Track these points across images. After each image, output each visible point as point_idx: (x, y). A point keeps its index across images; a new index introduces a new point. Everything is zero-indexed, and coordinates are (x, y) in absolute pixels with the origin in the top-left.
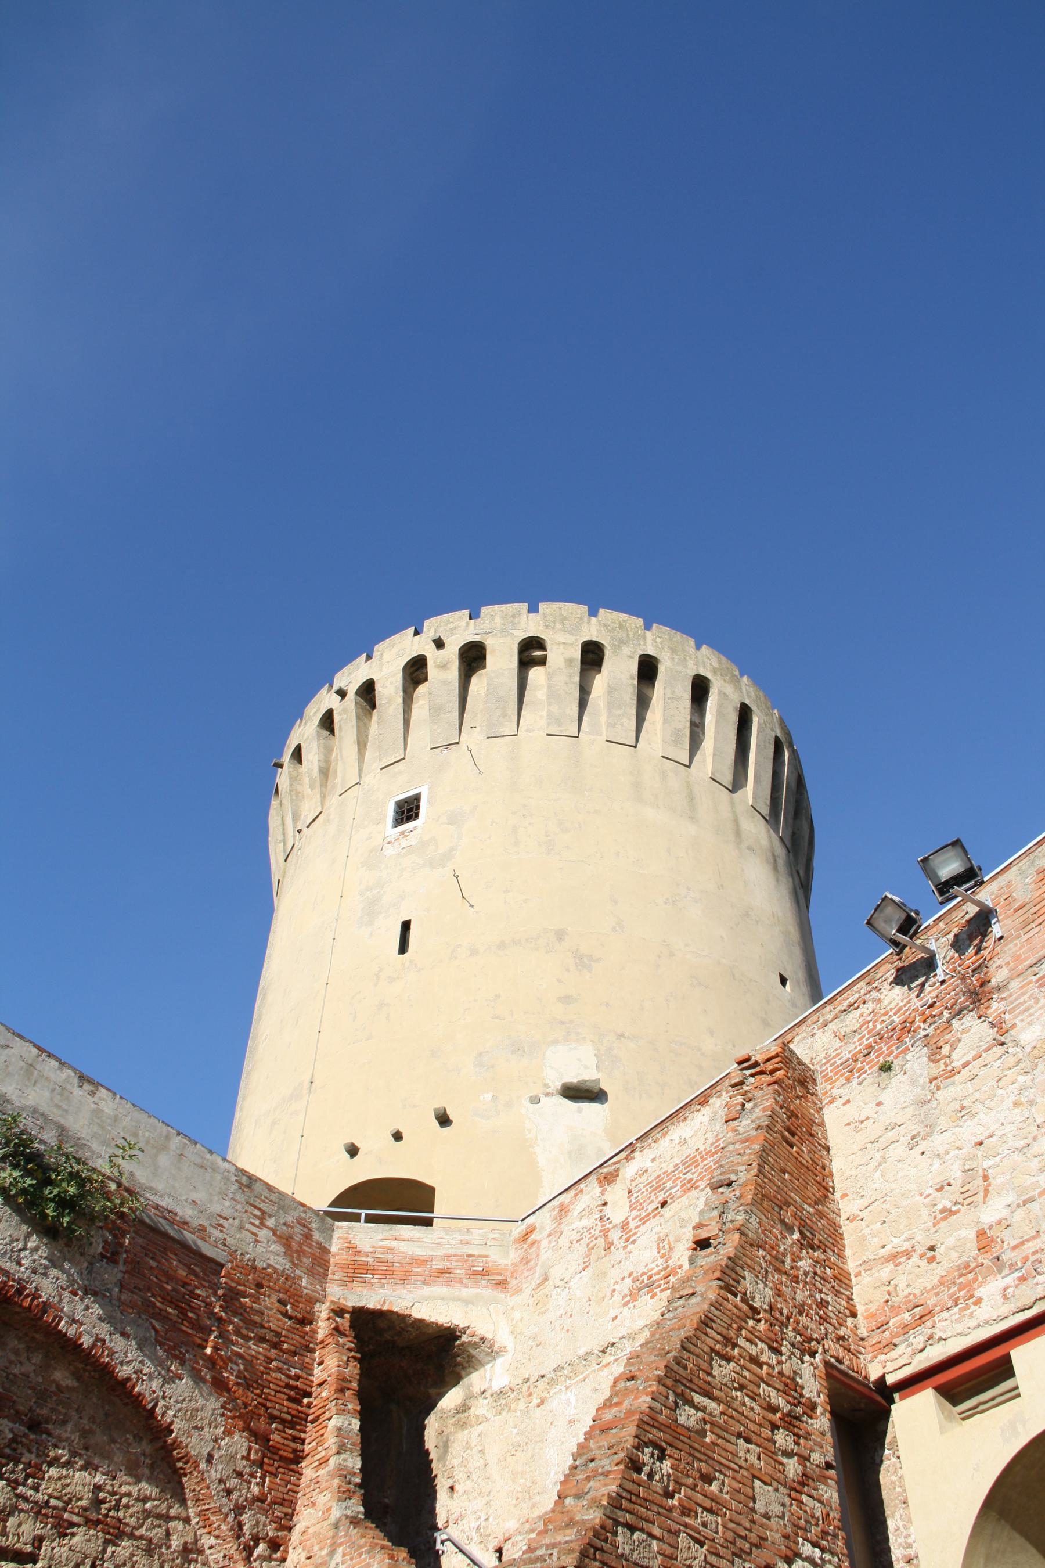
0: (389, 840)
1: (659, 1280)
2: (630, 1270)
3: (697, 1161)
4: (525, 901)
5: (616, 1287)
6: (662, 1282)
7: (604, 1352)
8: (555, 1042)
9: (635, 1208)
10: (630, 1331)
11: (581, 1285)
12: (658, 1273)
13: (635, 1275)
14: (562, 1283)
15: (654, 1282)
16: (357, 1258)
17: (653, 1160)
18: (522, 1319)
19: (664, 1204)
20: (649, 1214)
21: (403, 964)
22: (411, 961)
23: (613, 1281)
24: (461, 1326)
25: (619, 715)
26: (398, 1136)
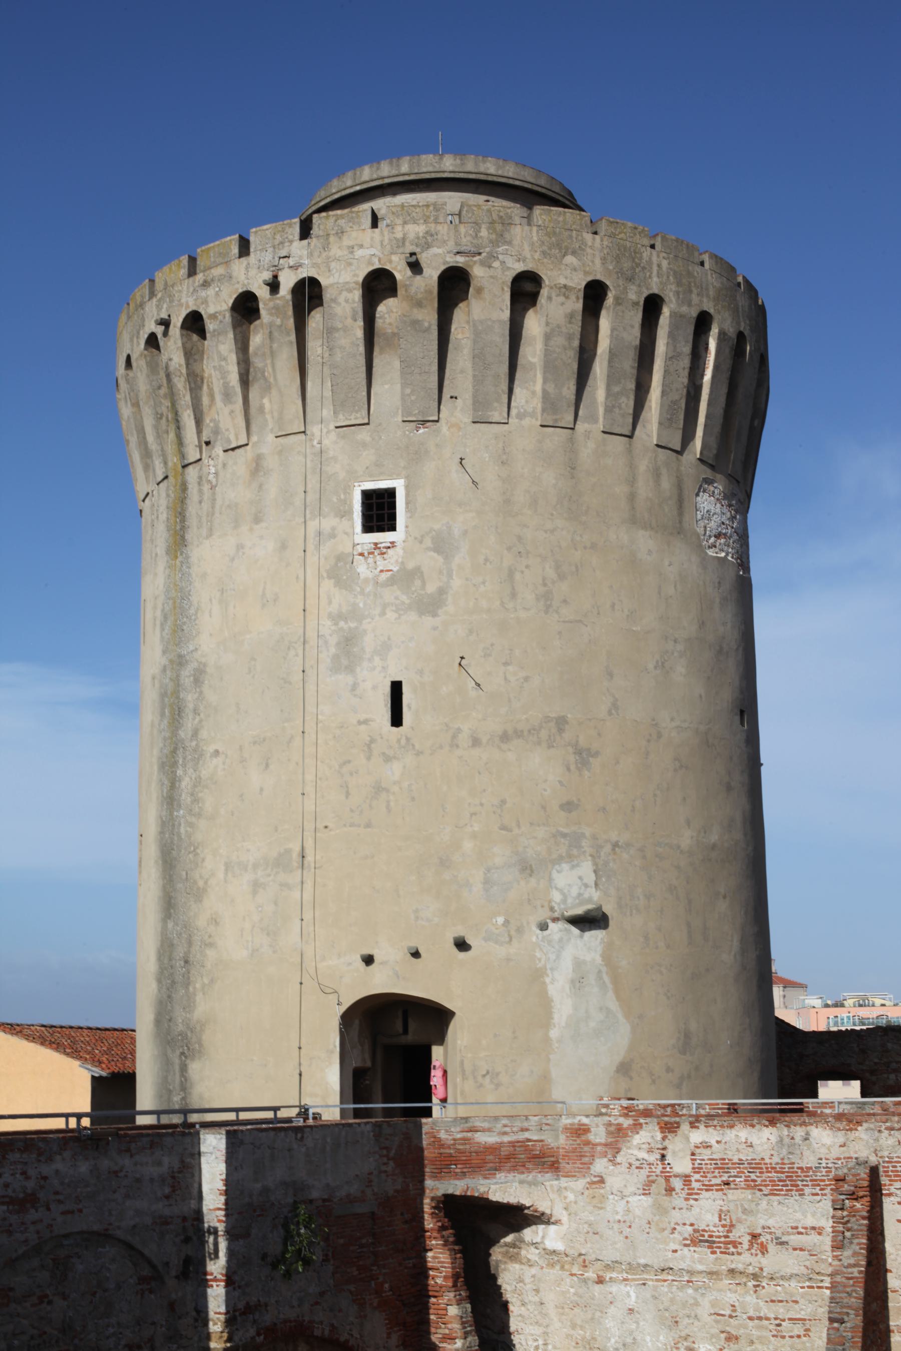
0: (359, 549)
1: (719, 1242)
2: (692, 1220)
3: (761, 1168)
4: (526, 679)
5: (676, 1227)
6: (722, 1245)
7: (663, 1270)
8: (560, 859)
9: (699, 1172)
11: (641, 1204)
12: (719, 1237)
14: (619, 1193)
15: (714, 1242)
16: (442, 1151)
17: (718, 1142)
18: (576, 1203)
19: (727, 1184)
20: (712, 1186)
21: (399, 741)
22: (408, 739)
26: (416, 954)
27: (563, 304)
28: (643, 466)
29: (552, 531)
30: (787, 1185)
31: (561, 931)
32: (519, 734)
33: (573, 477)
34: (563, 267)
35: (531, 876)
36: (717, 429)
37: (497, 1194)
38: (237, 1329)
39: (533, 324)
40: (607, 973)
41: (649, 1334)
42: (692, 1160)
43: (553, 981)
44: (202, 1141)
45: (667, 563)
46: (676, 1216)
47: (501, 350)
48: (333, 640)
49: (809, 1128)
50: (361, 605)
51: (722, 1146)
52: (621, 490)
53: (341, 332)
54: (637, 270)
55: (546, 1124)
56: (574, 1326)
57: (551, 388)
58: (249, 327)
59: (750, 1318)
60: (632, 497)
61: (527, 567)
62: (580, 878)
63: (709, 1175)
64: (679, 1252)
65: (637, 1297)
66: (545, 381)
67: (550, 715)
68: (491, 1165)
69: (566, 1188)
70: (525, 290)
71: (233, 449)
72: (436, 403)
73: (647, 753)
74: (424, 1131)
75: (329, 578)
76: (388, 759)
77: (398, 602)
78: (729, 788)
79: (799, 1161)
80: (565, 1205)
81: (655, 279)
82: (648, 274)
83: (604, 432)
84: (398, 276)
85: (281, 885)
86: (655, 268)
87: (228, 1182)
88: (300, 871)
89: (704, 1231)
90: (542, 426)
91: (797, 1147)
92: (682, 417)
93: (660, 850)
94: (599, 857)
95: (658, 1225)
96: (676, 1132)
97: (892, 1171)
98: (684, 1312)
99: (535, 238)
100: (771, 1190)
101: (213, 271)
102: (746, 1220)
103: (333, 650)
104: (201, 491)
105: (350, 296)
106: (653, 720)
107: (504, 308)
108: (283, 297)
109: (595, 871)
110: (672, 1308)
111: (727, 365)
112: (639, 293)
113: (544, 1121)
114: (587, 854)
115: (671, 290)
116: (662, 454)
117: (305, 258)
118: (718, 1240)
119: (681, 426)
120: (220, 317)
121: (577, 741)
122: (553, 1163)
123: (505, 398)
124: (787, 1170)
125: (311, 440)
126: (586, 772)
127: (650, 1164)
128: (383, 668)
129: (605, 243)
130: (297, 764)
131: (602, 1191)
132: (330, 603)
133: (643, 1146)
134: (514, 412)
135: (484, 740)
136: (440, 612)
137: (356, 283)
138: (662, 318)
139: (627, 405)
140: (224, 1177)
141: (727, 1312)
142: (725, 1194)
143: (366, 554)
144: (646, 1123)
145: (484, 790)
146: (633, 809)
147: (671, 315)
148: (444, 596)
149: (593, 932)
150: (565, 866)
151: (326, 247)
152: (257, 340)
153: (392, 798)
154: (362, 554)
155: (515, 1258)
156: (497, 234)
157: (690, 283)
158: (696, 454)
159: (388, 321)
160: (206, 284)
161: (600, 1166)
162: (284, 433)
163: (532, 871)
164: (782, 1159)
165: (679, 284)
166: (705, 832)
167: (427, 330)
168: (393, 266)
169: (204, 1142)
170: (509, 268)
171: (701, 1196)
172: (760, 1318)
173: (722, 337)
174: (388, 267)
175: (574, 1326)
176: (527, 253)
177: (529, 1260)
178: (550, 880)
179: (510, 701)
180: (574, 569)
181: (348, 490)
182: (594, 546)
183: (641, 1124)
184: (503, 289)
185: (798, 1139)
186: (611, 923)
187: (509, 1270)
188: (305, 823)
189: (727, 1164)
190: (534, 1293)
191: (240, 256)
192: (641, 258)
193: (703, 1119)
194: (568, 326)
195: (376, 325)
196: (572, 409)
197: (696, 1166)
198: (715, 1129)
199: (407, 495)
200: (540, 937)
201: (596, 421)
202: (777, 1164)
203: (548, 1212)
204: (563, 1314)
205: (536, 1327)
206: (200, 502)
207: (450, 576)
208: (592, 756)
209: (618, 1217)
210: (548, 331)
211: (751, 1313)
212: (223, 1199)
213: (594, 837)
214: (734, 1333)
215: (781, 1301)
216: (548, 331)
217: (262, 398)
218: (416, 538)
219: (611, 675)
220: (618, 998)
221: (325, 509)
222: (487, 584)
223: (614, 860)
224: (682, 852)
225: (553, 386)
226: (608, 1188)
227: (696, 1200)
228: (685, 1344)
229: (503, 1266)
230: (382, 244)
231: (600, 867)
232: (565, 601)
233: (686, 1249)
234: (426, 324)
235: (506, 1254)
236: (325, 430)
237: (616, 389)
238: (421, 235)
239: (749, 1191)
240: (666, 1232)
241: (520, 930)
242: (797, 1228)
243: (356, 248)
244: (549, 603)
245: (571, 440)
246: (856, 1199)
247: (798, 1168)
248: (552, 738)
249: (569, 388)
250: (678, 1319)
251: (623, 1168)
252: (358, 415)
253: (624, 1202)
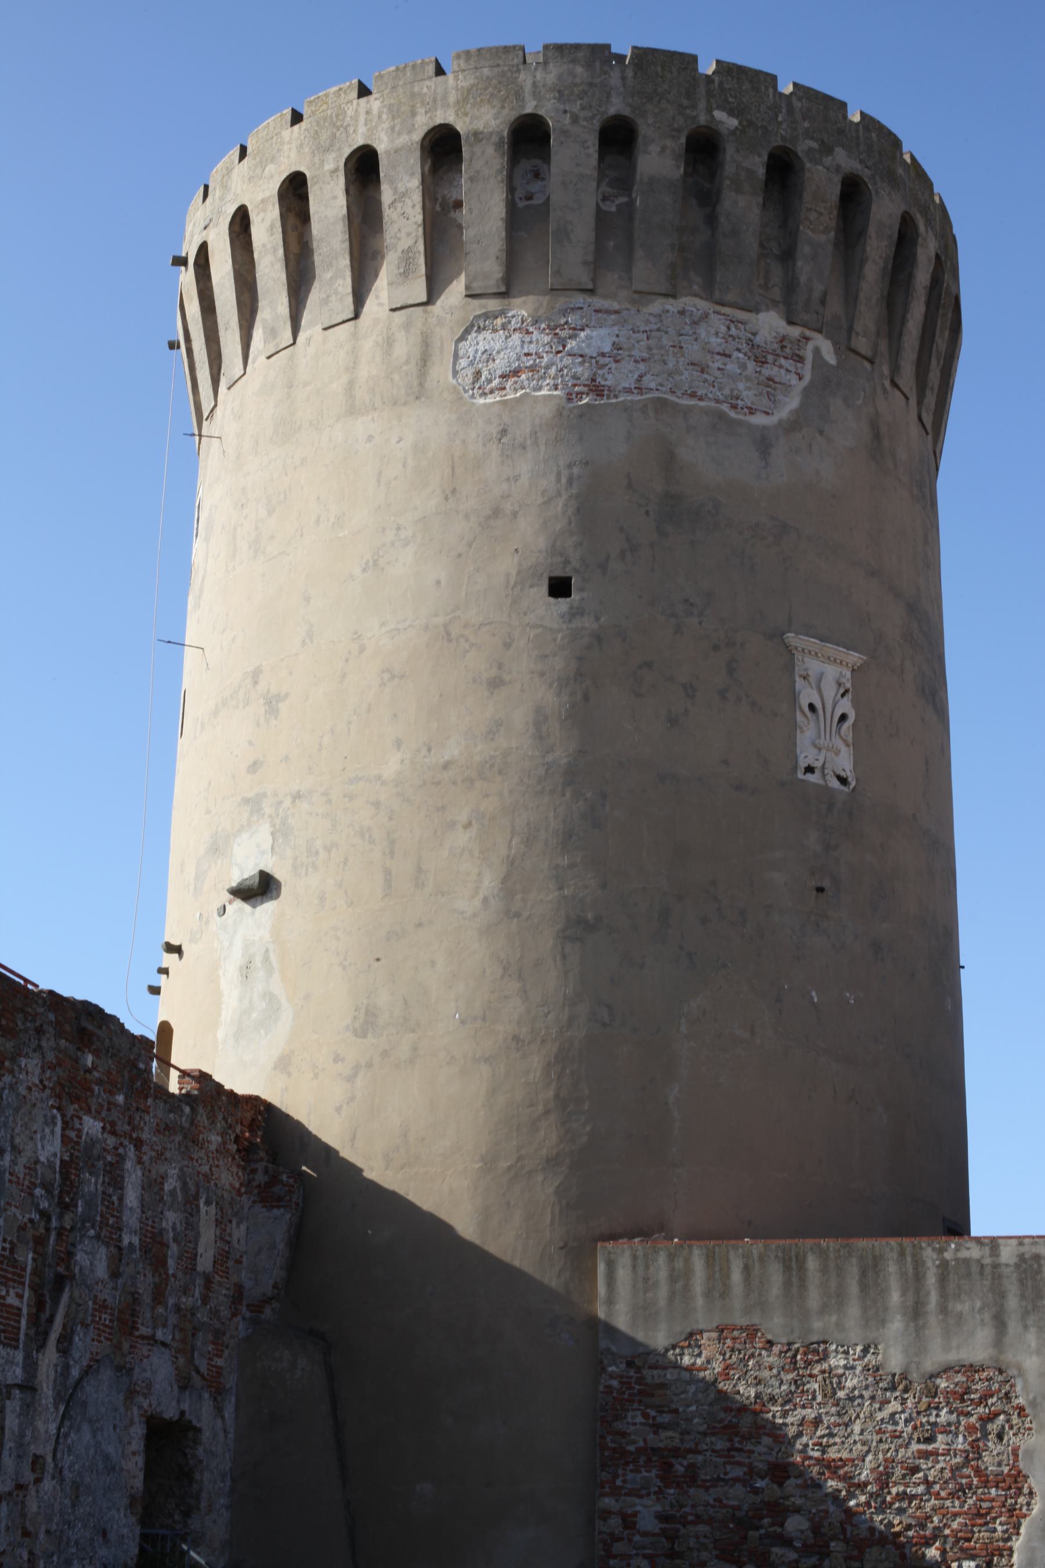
25: (331, 278)
28: (368, 345)
73: (344, 676)
86: (362, 118)
92: (422, 261)
109: (272, 834)
166: (429, 750)
182: (303, 461)
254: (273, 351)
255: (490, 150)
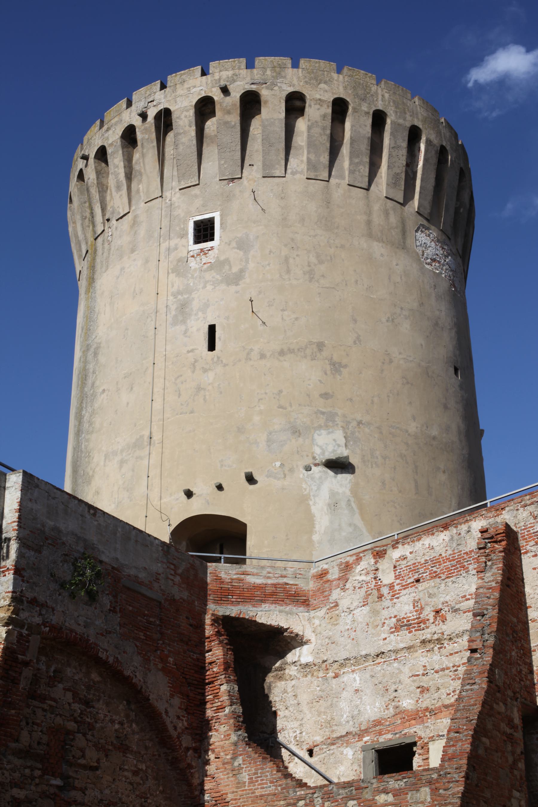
0: (191, 254)
1: (414, 624)
3: (440, 562)
4: (297, 319)
5: (385, 621)
6: (416, 625)
7: (378, 656)
8: (320, 427)
9: (399, 578)
10: (395, 648)
11: (362, 614)
12: (414, 620)
13: (398, 617)
14: (348, 610)
15: (411, 624)
16: (222, 586)
17: (411, 553)
18: (320, 625)
19: (418, 581)
21: (213, 359)
22: (218, 358)
23: (384, 617)
24: (285, 627)
25: (357, 163)
26: (220, 487)
27: (319, 109)
28: (376, 207)
29: (315, 236)
30: (457, 568)
31: (320, 472)
32: (291, 351)
33: (328, 207)
34: (318, 90)
35: (299, 436)
36: (430, 197)
37: (263, 618)
38: (23, 609)
39: (301, 125)
40: (354, 502)
41: (369, 704)
42: (394, 571)
43: (315, 504)
44: (7, 480)
45: (394, 263)
46: (385, 613)
47: (280, 135)
48: (173, 307)
49: (470, 523)
50: (192, 284)
51: (414, 554)
52: (362, 218)
53: (183, 135)
54: (368, 96)
55: (300, 574)
56: (319, 714)
57: (312, 157)
58: (133, 151)
59: (437, 672)
60: (369, 223)
61: (297, 255)
62: (334, 440)
63: (405, 578)
64: (388, 639)
65: (361, 680)
66: (309, 153)
67: (313, 340)
68: (258, 598)
69: (313, 617)
70: (295, 104)
71: (121, 218)
72: (240, 168)
73: (382, 370)
74: (208, 572)
75: (173, 272)
76: (205, 371)
77: (214, 279)
78: (446, 407)
79: (465, 548)
80: (313, 629)
81: (380, 102)
82: (375, 99)
83: (349, 185)
84: (216, 98)
85: (137, 458)
86: (380, 97)
87: (21, 504)
88: (149, 446)
89: (404, 618)
90: (307, 179)
91: (463, 539)
93: (393, 430)
94: (348, 429)
95: (373, 624)
96: (384, 556)
97: (527, 535)
98: (392, 681)
99: (301, 75)
100: (447, 575)
101: (112, 121)
102: (431, 602)
103: (173, 313)
104: (103, 248)
105: (187, 114)
106: (386, 351)
107: (281, 111)
108: (150, 122)
109: (345, 437)
110: (384, 681)
111: (434, 160)
112: (369, 107)
113: (298, 572)
114: (339, 426)
115: (391, 109)
116: (390, 203)
117: (163, 99)
118: (413, 622)
119: (403, 189)
120: (115, 144)
121: (332, 358)
122: (305, 601)
123: (283, 163)
124: (457, 557)
125: (165, 200)
126: (338, 376)
127: (367, 583)
128: (204, 318)
129: (346, 79)
130: (149, 383)
131: (337, 612)
132: (173, 286)
133: (363, 572)
134: (289, 171)
135: (268, 355)
136: (240, 282)
137: (191, 106)
138: (386, 126)
139: (364, 170)
140: (19, 500)
141: (421, 673)
142: (417, 588)
143: (195, 256)
144: (364, 556)
145: (268, 385)
146: (373, 402)
147: (391, 123)
148: (244, 273)
149: (344, 475)
150: (323, 432)
151: (174, 91)
152: (137, 156)
153: (207, 393)
154: (193, 256)
155: (280, 678)
156: (277, 73)
157: (404, 109)
158: (415, 209)
159: (212, 129)
160: (107, 130)
161: (336, 594)
162: (150, 199)
163: (300, 434)
164: (453, 550)
165: (397, 107)
166: (427, 427)
167: (234, 127)
168: (213, 93)
169: (9, 481)
170: (284, 90)
171: (401, 594)
172: (443, 670)
173: (429, 143)
174: (210, 95)
175: (319, 714)
176: (295, 81)
177: (291, 676)
178: (313, 439)
179: (285, 331)
180: (329, 258)
181: (186, 222)
183: (361, 558)
184: (280, 101)
185: (463, 534)
186: (356, 470)
187: (277, 686)
188: (153, 417)
189: (418, 566)
190: (294, 698)
191: (127, 108)
192: (370, 90)
193: (401, 540)
194: (323, 122)
195: (205, 132)
196: (327, 170)
197: (397, 574)
198: (409, 545)
199: (221, 220)
200: (306, 475)
201: (344, 179)
202: (450, 555)
203: (301, 633)
204: (312, 707)
205: (295, 722)
206: (103, 254)
207: (247, 261)
208: (343, 367)
209: (348, 627)
210: (310, 124)
211: (437, 667)
212: (17, 514)
213: (344, 416)
214: (426, 686)
215: (457, 653)
216: (310, 124)
217: (138, 185)
218: (226, 243)
219: (355, 321)
220: (363, 519)
221: (172, 235)
222: (271, 265)
223: (359, 432)
224: (409, 435)
225: (314, 156)
226: (341, 609)
227: (398, 598)
228: (393, 704)
229: (274, 685)
230: (207, 83)
231: (348, 435)
232: (323, 276)
233: (392, 635)
234: (233, 123)
235: (275, 677)
236: (173, 193)
237: (357, 160)
238: (230, 76)
239: (432, 581)
240: (379, 627)
241: (291, 470)
242: (465, 596)
243: (191, 88)
244: (312, 276)
245: (327, 187)
246: (496, 542)
247: (464, 554)
248: (314, 354)
249: (324, 157)
250: (388, 687)
251: (350, 591)
252: (193, 180)
253: (351, 615)
254: (313, 178)
255: (433, 152)
